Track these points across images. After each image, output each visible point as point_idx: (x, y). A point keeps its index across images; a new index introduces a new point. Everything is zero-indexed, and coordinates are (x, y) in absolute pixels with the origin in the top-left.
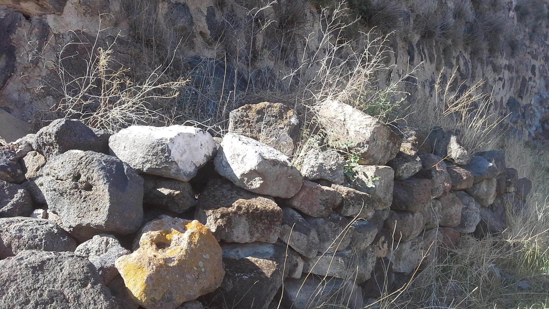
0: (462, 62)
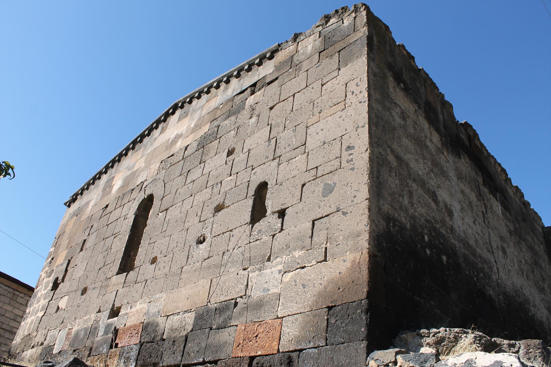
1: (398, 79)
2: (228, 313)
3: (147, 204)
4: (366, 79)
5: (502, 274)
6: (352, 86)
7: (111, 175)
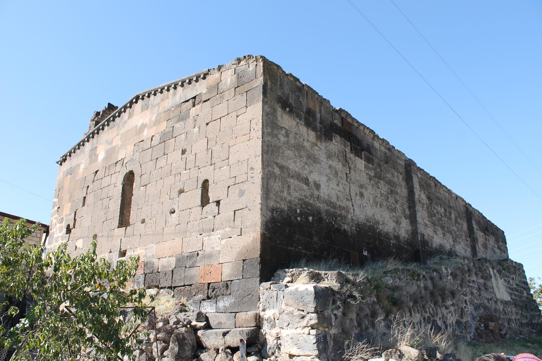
0: (431, 309)
1: (285, 104)
2: (194, 259)
3: (129, 178)
4: (261, 121)
5: (357, 212)
6: (253, 125)
7: (93, 144)
